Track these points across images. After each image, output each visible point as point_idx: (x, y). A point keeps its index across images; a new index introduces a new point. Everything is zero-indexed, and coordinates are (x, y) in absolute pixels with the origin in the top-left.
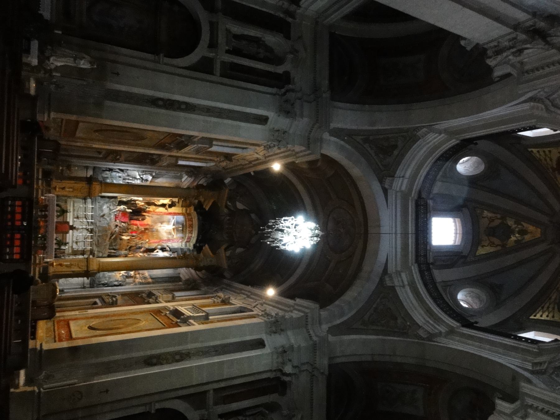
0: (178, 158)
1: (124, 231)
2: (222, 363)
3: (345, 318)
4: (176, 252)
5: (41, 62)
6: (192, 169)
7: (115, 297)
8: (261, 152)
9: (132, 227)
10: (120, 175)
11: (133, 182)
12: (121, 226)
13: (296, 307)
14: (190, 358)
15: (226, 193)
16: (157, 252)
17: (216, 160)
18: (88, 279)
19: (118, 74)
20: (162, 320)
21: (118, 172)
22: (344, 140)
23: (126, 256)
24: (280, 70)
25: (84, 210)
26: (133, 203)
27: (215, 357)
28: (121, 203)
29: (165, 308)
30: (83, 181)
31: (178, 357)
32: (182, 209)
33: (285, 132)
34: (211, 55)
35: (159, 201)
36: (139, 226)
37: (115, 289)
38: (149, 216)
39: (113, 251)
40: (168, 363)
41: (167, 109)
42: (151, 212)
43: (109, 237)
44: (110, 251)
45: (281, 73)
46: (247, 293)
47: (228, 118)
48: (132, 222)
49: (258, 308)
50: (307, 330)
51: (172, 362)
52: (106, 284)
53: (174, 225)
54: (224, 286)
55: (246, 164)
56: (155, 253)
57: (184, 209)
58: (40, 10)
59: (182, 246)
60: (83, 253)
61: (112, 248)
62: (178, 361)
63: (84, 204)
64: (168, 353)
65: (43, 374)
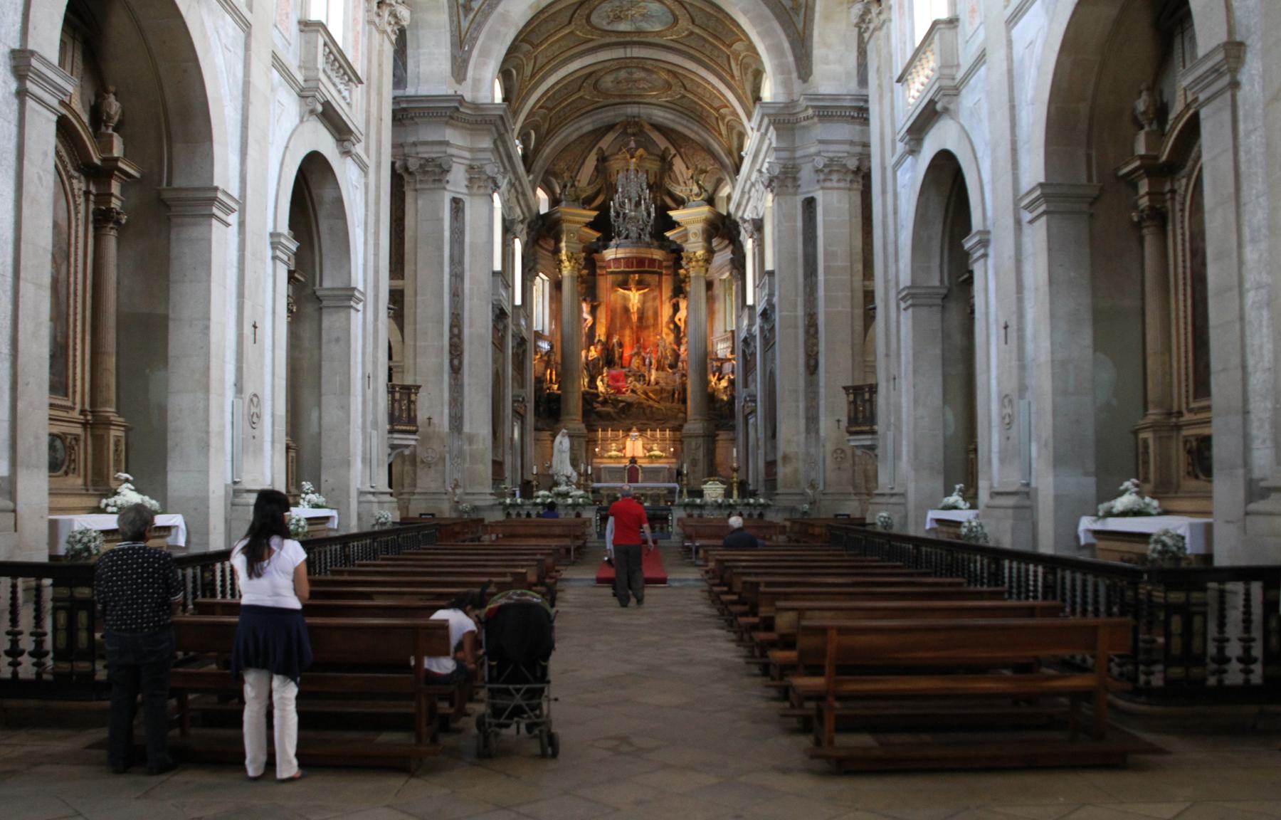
2: (827, 269)
3: (787, 45)
6: (527, 270)
7: (745, 398)
16: (680, 320)
18: (717, 435)
19: (429, 419)
23: (684, 375)
29: (762, 328)
31: (812, 330)
33: (471, 167)
35: (586, 320)
36: (633, 352)
39: (676, 396)
40: (816, 344)
44: (676, 401)
47: (461, 263)
48: (625, 362)
51: (817, 338)
53: (629, 289)
54: (740, 214)
55: (516, 191)
56: (682, 325)
57: (598, 271)
62: (816, 332)
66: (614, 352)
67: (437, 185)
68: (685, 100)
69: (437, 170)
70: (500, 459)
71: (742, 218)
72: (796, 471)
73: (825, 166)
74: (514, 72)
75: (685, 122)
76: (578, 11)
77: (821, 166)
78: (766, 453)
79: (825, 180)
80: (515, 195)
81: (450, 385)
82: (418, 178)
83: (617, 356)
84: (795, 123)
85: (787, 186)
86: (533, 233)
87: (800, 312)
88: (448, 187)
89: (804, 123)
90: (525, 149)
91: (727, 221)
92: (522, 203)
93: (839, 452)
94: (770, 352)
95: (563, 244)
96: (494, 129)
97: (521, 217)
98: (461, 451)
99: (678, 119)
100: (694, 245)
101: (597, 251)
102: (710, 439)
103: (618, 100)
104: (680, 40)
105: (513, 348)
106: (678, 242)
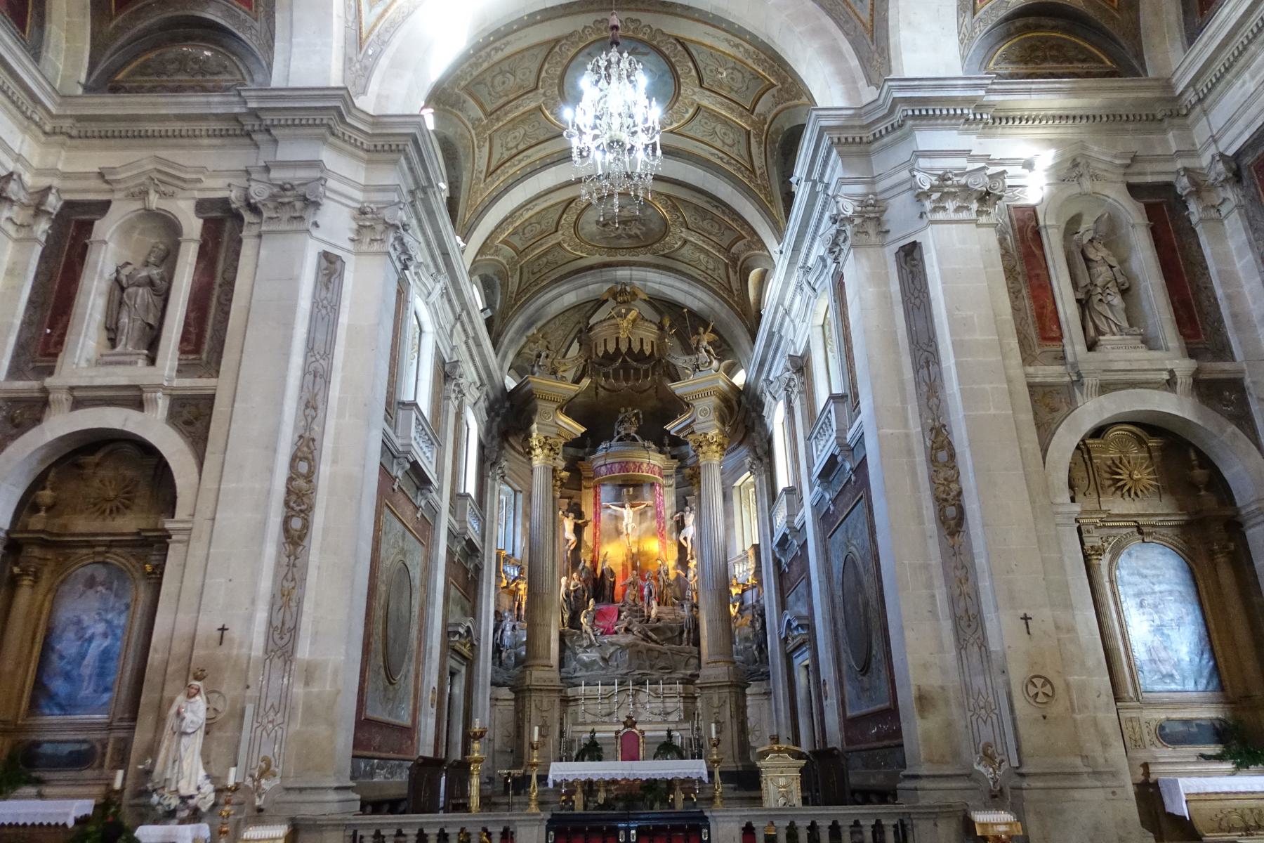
0: (458, 498)
1: (638, 613)
2: (958, 346)
3: (846, 46)
4: (684, 497)
5: (196, 816)
6: (488, 464)
7: (789, 623)
8: (424, 285)
9: (629, 599)
10: (508, 628)
11: (525, 598)
12: (627, 620)
13: (815, 176)
14: (944, 426)
15: (540, 382)
16: (685, 539)
17: (456, 403)
20: (848, 506)
21: (502, 632)
22: (376, 57)
23: (695, 606)
24: (193, 226)
25: (593, 702)
26: (575, 597)
27: (944, 365)
28: (574, 622)
29: (816, 507)
30: (524, 706)
31: (943, 456)
32: (586, 488)
33: (363, 212)
34: (163, 404)
35: (568, 541)
37: (772, 624)
38: (604, 562)
39: (685, 635)
41: (311, 508)
42: (594, 556)
43: (652, 645)
45: (201, 221)
46: (779, 317)
47: (328, 354)
49: (817, 279)
50: (876, 139)
52: (759, 646)
53: (623, 506)
54: (763, 376)
55: (465, 330)
57: (585, 483)
58: (65, 825)
59: (671, 486)
60: (690, 699)
61: (677, 639)
62: (952, 456)
63: (580, 702)
64: (932, 481)
65: (981, 768)
66: (604, 585)
67: (296, 225)
68: (687, 247)
69: (298, 205)
70: (406, 720)
71: (767, 379)
72: (949, 725)
73: (933, 188)
74: (498, 282)
75: (685, 287)
76: (546, 66)
77: (927, 187)
78: (842, 704)
79: (934, 210)
80: (464, 339)
81: (278, 564)
82: (265, 215)
83: (608, 584)
84: (869, 143)
85: (866, 233)
86: (499, 419)
87: (915, 428)
88: (315, 232)
89: (886, 140)
90: (489, 304)
91: (743, 399)
92: (477, 360)
93: (1039, 682)
94: (839, 535)
95: (535, 426)
96: (402, 158)
97: (478, 384)
98: (285, 696)
99: (678, 284)
100: (703, 425)
101: (583, 459)
102: (738, 687)
103: (606, 259)
104: (682, 130)
105: (450, 553)
106: (681, 435)
